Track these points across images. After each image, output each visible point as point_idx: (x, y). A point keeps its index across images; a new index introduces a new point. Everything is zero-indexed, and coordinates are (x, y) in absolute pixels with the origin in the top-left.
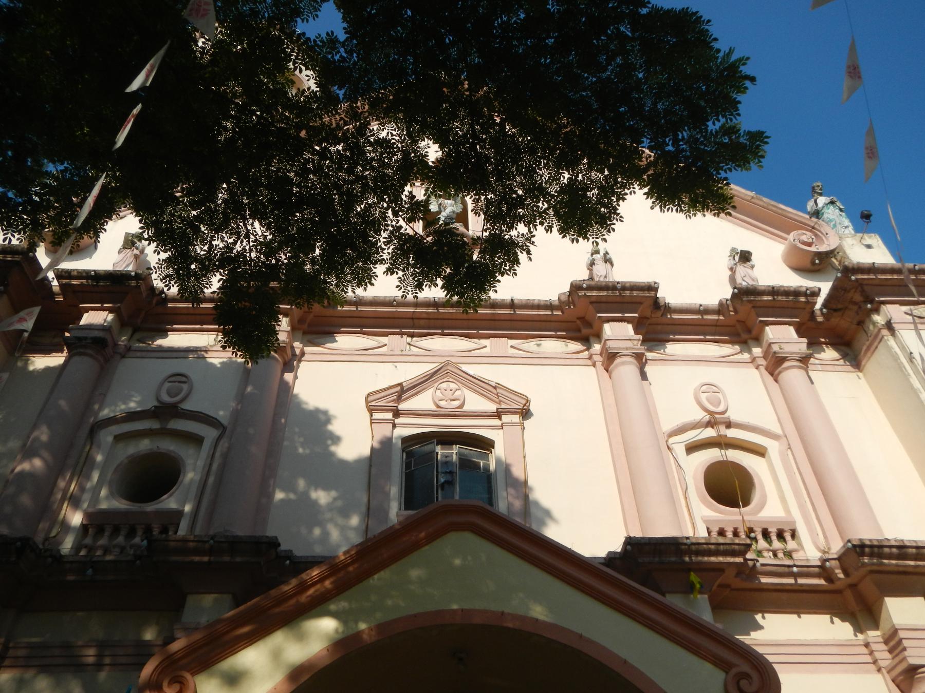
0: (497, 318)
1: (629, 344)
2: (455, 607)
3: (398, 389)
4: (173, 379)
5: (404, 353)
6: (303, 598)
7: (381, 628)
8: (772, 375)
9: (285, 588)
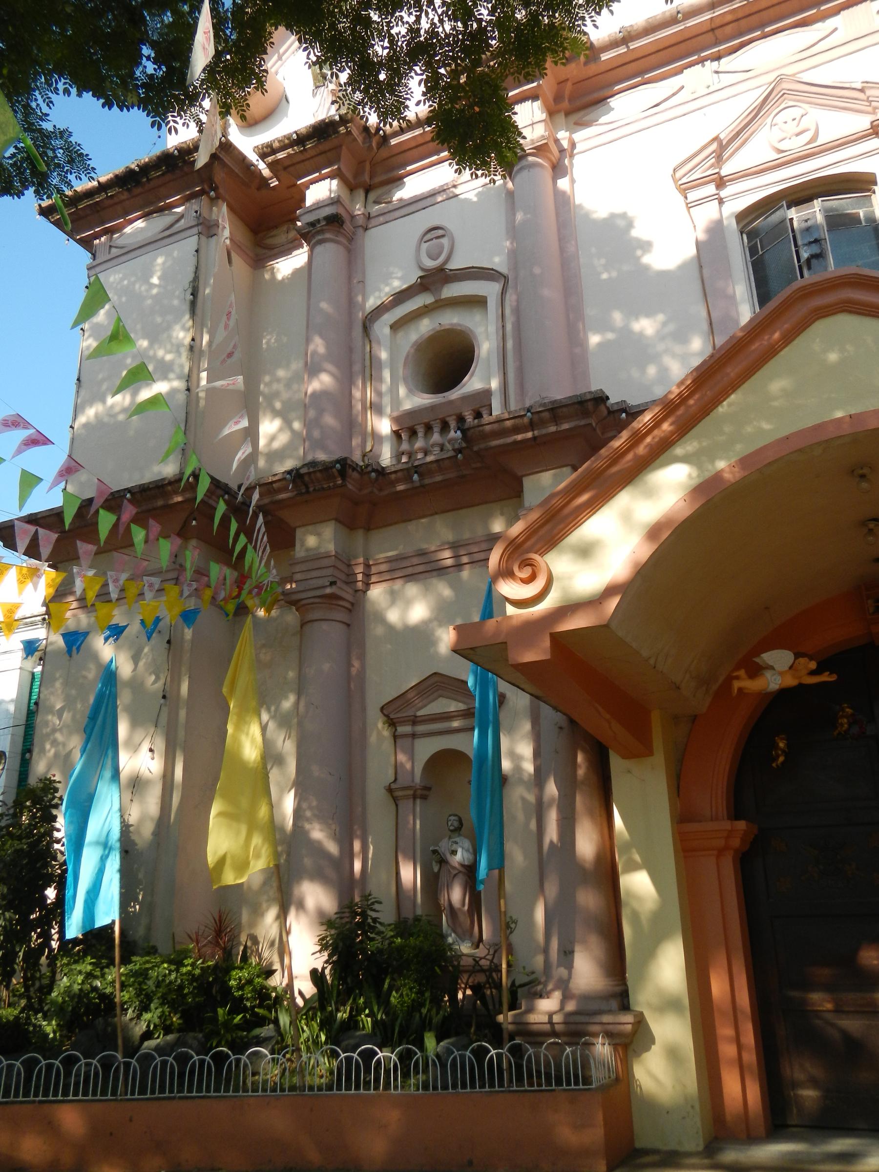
2: (839, 414)
3: (714, 146)
4: (429, 236)
5: (711, 89)
6: (641, 450)
7: (743, 462)
9: (616, 443)
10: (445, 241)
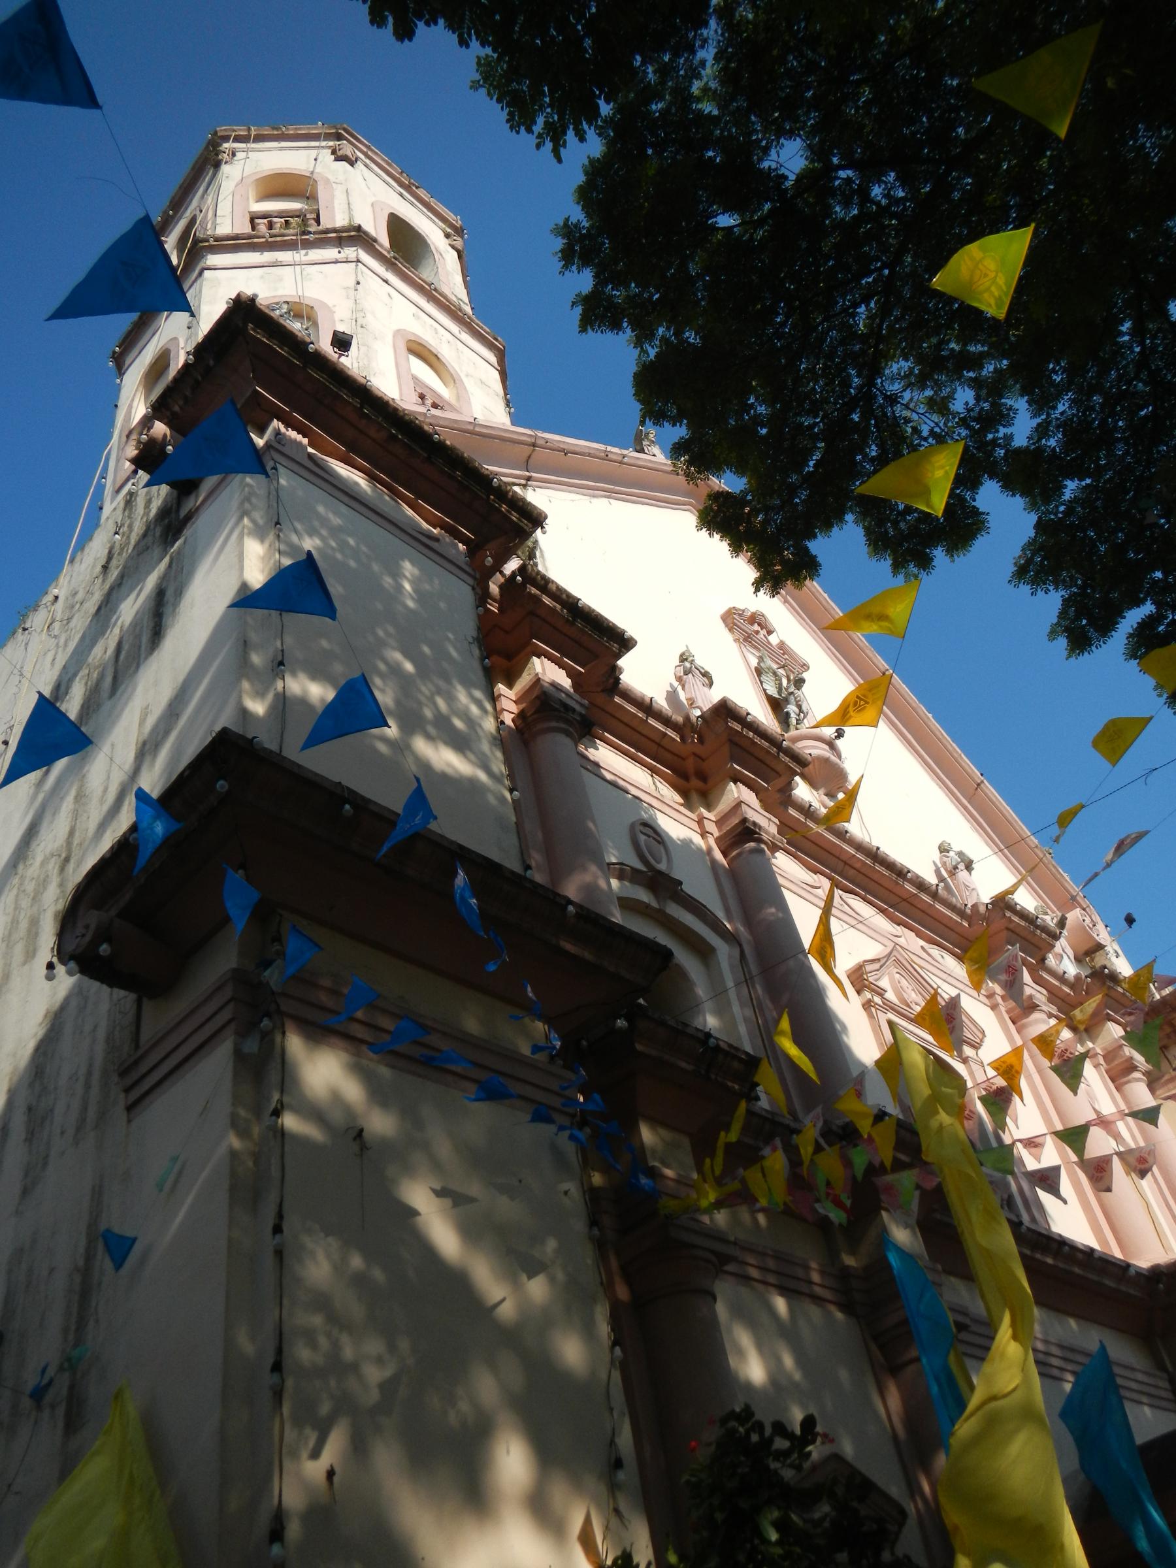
0: (915, 902)
8: (1113, 1081)
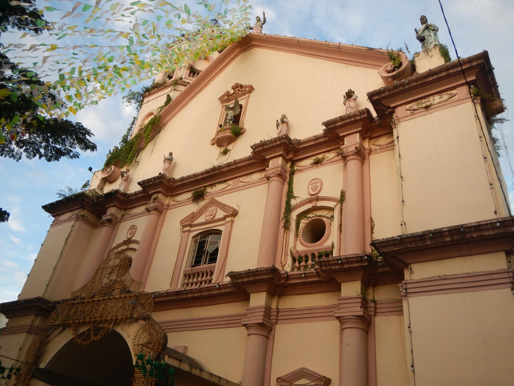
1: (275, 170)
10: (134, 230)
